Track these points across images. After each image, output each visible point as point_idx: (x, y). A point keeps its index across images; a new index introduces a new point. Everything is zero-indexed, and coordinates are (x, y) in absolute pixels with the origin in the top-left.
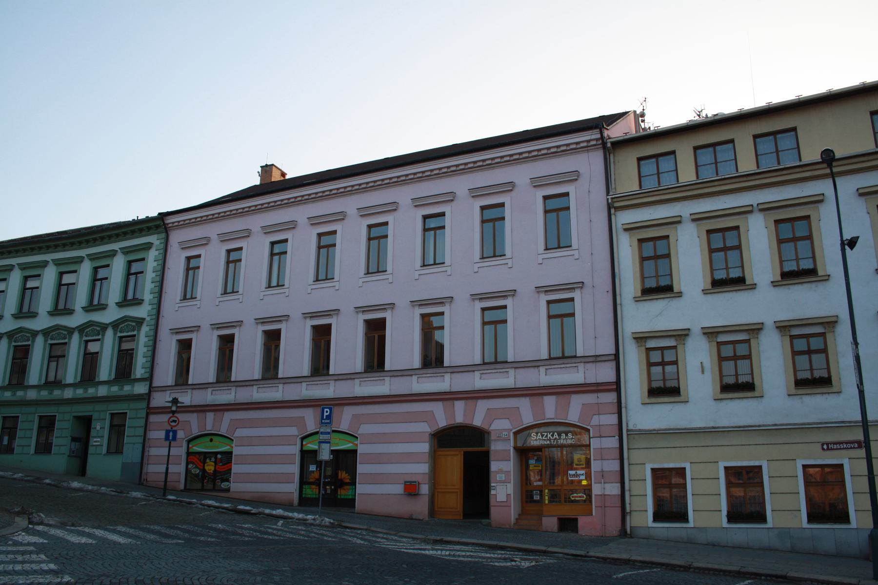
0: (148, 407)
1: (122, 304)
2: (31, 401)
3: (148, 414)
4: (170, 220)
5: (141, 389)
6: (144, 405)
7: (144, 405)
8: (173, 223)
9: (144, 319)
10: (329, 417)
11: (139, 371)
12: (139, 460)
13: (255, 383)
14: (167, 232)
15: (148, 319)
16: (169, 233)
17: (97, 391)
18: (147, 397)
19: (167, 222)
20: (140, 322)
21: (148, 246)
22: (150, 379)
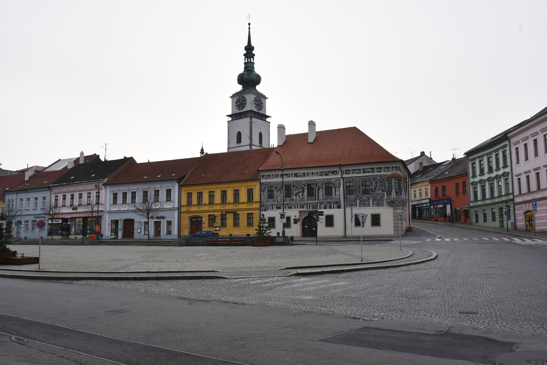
0: (514, 203)
1: (504, 168)
2: (488, 204)
3: (514, 205)
4: (509, 135)
5: (511, 197)
6: (512, 202)
7: (512, 202)
8: (510, 136)
9: (509, 172)
10: (535, 205)
11: (511, 191)
12: (514, 221)
13: (536, 192)
14: (509, 140)
15: (510, 172)
16: (510, 139)
17: (502, 198)
18: (513, 200)
19: (508, 136)
20: (508, 173)
21: (506, 146)
22: (513, 193)
